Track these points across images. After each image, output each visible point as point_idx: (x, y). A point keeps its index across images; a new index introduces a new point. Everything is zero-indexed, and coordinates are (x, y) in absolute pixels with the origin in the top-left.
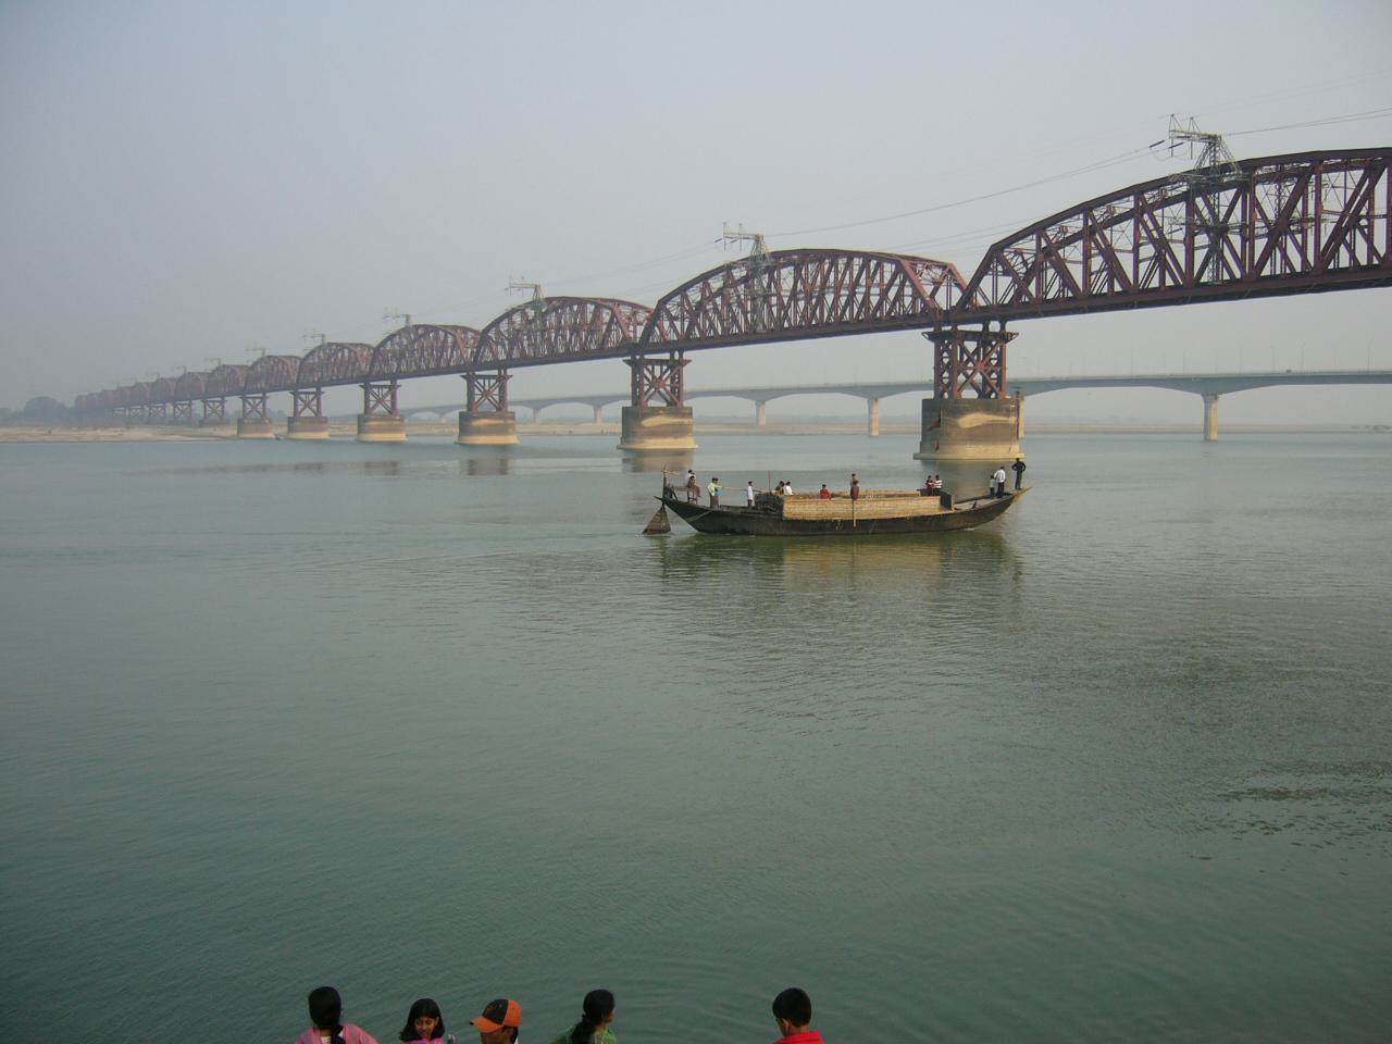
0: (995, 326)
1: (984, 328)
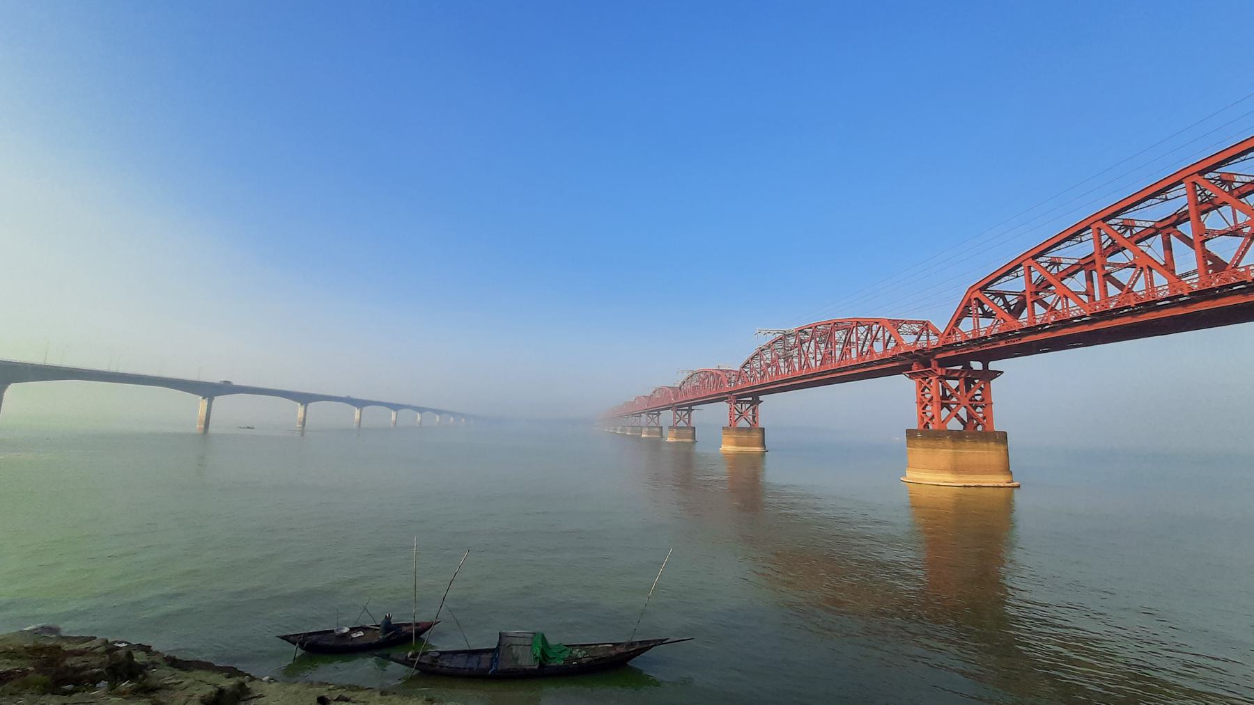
0: (977, 366)
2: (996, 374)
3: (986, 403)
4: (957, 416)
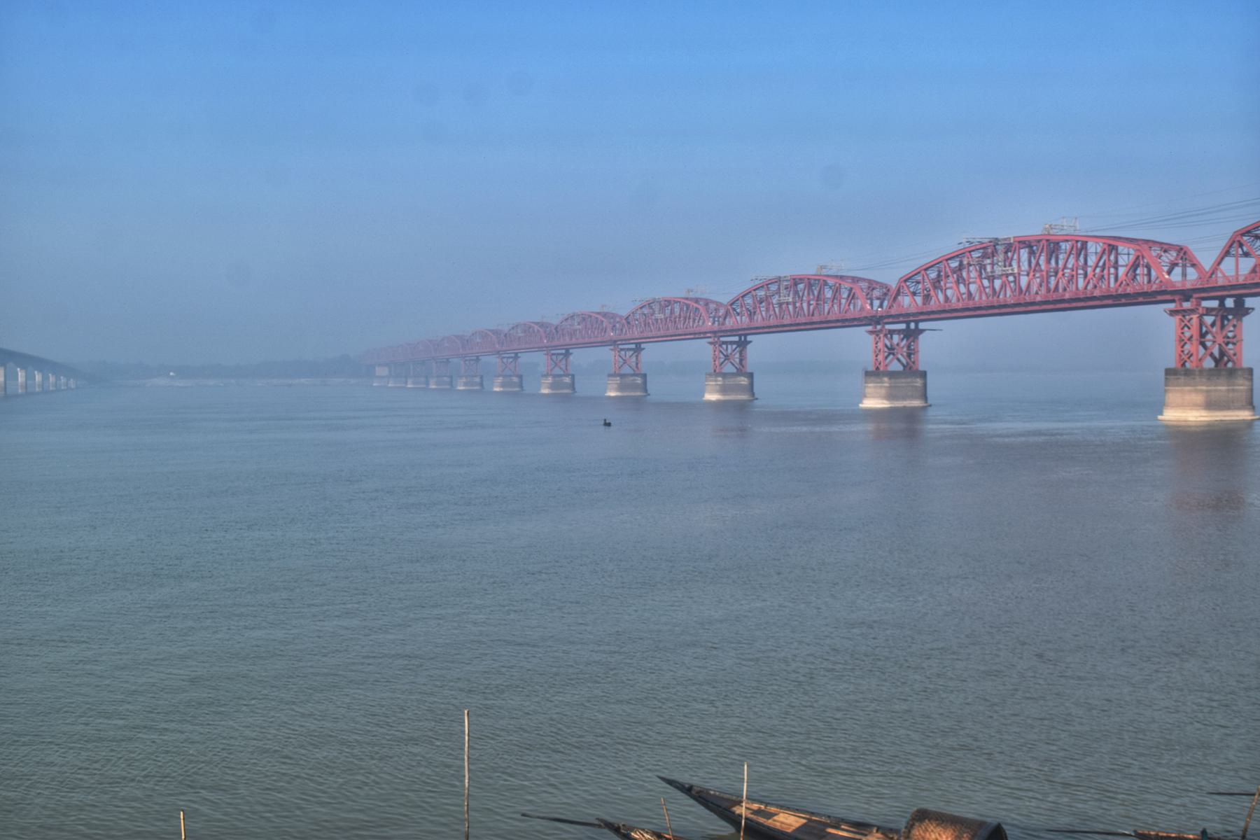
0: (912, 326)
2: (922, 331)
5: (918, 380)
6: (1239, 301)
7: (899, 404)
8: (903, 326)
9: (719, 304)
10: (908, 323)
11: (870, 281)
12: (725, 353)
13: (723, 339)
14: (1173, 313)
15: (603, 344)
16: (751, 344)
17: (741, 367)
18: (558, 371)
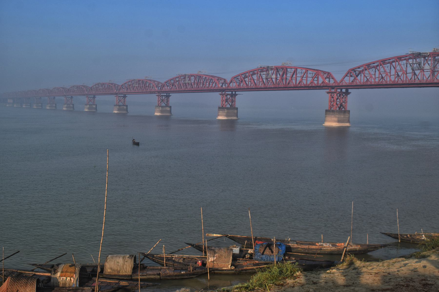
0: (234, 93)
1: (232, 93)
2: (237, 95)
3: (235, 101)
4: (229, 104)
5: (236, 110)
6: (347, 90)
7: (230, 118)
8: (230, 93)
9: (159, 83)
10: (232, 92)
11: (218, 77)
12: (162, 99)
13: (161, 94)
14: (328, 93)
15: (112, 94)
16: (171, 96)
17: (167, 104)
18: (91, 103)
